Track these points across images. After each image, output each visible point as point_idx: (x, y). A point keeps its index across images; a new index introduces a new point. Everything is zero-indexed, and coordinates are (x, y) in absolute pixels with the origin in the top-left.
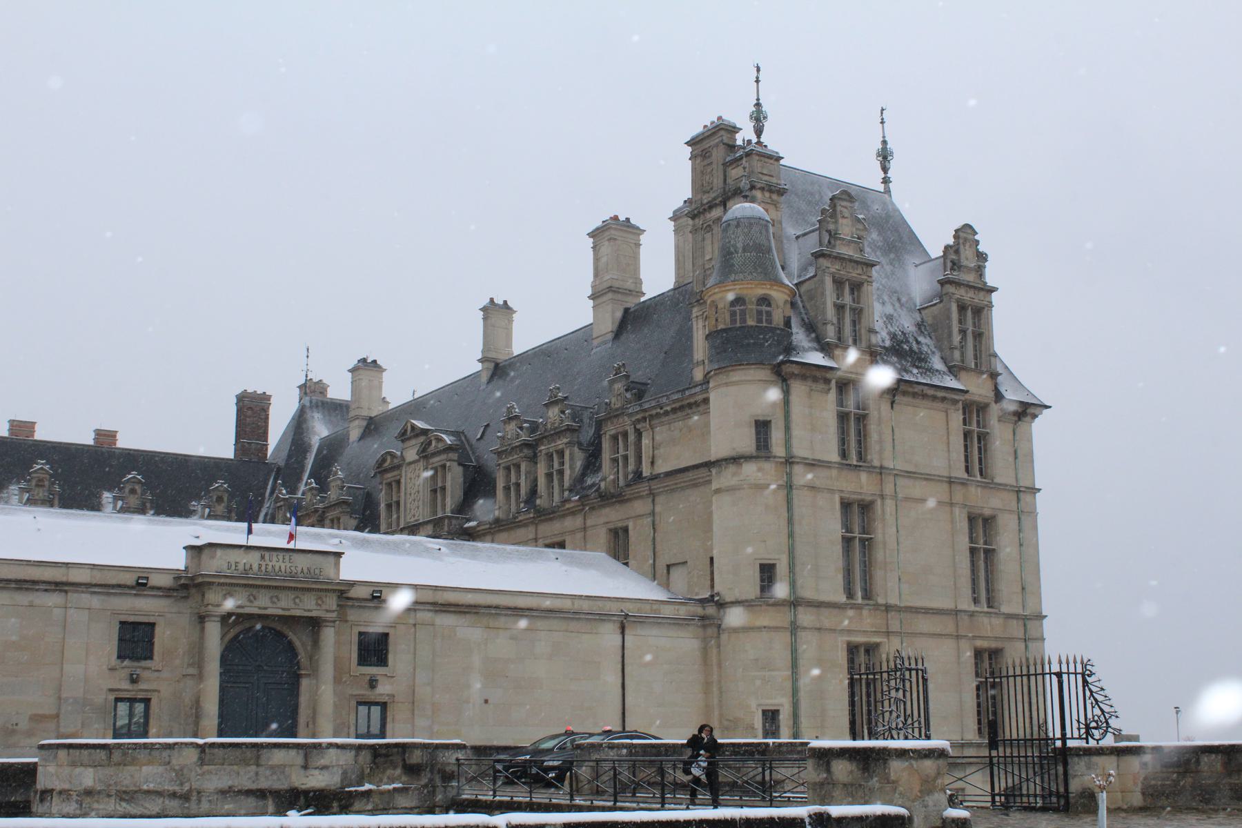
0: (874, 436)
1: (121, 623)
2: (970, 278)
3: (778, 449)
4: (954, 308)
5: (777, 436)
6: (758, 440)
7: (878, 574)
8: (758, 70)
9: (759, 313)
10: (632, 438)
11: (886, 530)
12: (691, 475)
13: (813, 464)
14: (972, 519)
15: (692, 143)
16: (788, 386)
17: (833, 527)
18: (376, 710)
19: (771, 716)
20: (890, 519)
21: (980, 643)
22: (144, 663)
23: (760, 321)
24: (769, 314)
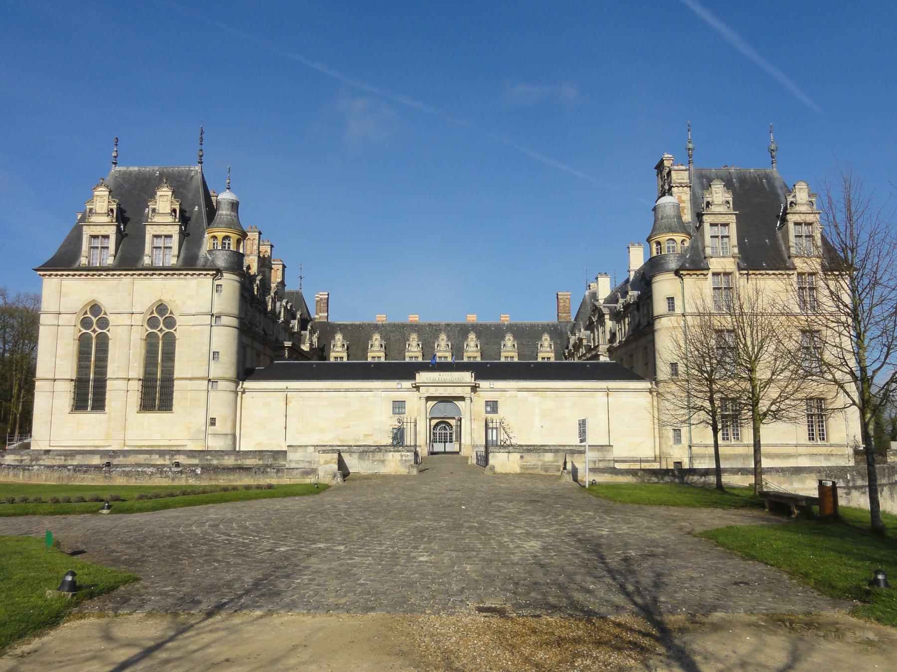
3: (678, 310)
5: (678, 303)
6: (669, 307)
9: (669, 247)
15: (656, 168)
16: (682, 280)
18: (495, 431)
23: (669, 251)
24: (673, 247)
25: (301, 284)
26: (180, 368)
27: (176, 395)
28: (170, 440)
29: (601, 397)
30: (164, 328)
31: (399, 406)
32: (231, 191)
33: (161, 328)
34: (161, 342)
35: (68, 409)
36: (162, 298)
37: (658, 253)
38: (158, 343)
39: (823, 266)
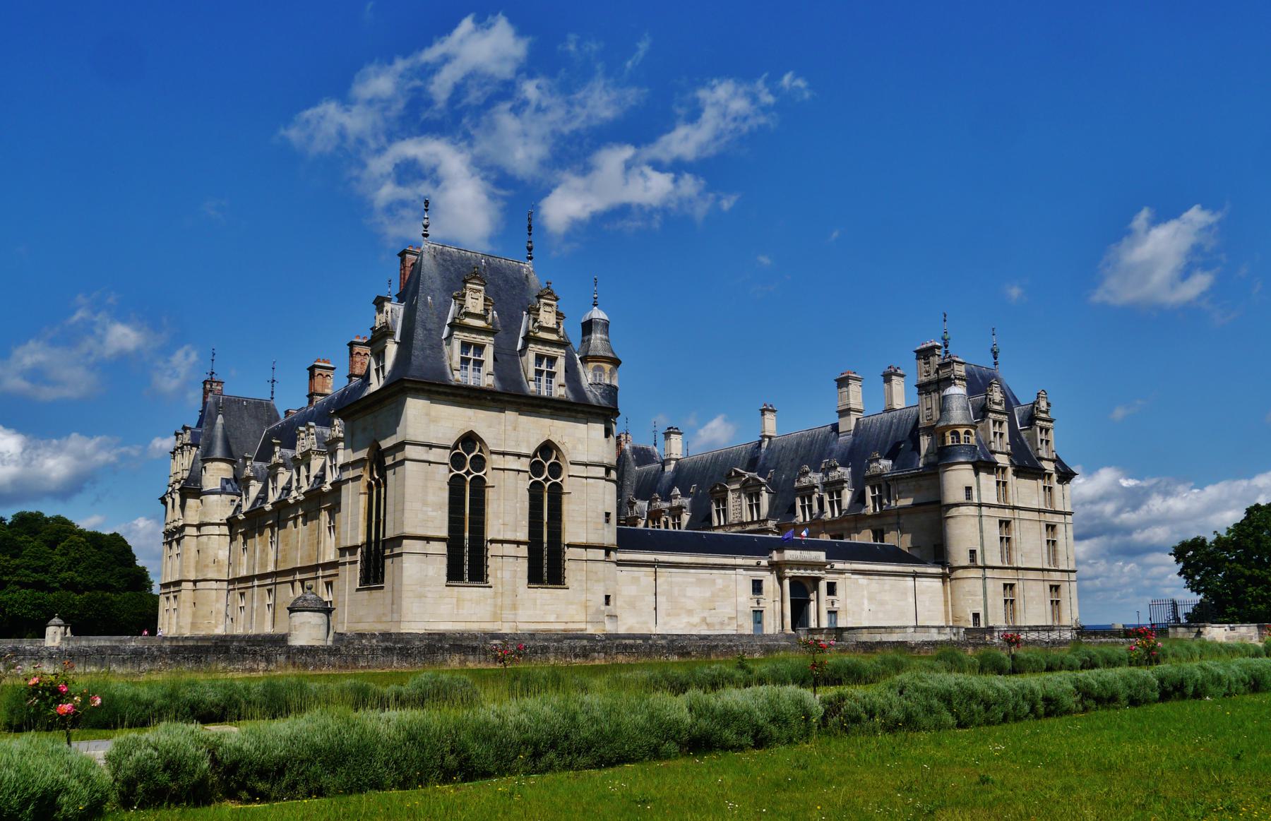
0: (1010, 492)
1: (753, 580)
2: (1043, 415)
4: (1038, 429)
5: (975, 493)
7: (1014, 553)
8: (945, 316)
10: (884, 487)
11: (1015, 535)
12: (922, 508)
13: (990, 506)
14: (1048, 526)
17: (993, 531)
19: (976, 616)
20: (1018, 529)
21: (1052, 583)
22: (760, 596)
24: (968, 438)
25: (272, 392)
26: (572, 531)
27: (568, 565)
28: (566, 623)
29: (910, 581)
30: (544, 477)
31: (757, 587)
32: (599, 309)
33: (547, 477)
34: (546, 495)
35: (446, 578)
36: (550, 438)
37: (953, 442)
38: (543, 496)
39: (1056, 468)
